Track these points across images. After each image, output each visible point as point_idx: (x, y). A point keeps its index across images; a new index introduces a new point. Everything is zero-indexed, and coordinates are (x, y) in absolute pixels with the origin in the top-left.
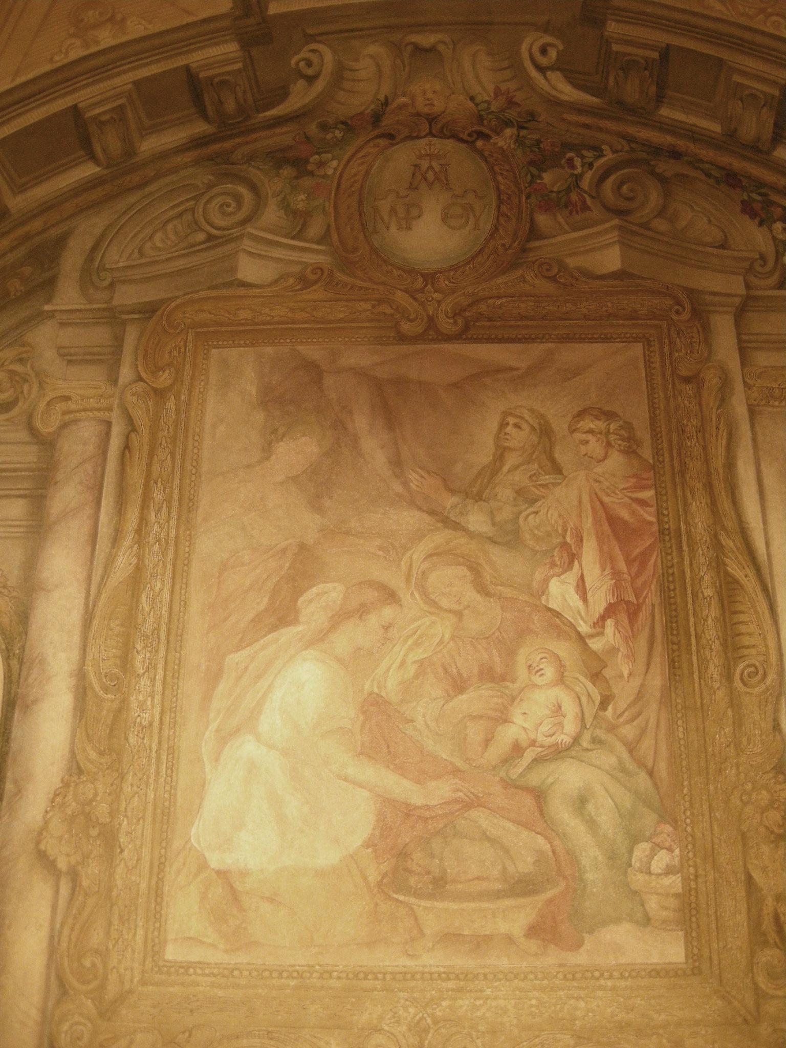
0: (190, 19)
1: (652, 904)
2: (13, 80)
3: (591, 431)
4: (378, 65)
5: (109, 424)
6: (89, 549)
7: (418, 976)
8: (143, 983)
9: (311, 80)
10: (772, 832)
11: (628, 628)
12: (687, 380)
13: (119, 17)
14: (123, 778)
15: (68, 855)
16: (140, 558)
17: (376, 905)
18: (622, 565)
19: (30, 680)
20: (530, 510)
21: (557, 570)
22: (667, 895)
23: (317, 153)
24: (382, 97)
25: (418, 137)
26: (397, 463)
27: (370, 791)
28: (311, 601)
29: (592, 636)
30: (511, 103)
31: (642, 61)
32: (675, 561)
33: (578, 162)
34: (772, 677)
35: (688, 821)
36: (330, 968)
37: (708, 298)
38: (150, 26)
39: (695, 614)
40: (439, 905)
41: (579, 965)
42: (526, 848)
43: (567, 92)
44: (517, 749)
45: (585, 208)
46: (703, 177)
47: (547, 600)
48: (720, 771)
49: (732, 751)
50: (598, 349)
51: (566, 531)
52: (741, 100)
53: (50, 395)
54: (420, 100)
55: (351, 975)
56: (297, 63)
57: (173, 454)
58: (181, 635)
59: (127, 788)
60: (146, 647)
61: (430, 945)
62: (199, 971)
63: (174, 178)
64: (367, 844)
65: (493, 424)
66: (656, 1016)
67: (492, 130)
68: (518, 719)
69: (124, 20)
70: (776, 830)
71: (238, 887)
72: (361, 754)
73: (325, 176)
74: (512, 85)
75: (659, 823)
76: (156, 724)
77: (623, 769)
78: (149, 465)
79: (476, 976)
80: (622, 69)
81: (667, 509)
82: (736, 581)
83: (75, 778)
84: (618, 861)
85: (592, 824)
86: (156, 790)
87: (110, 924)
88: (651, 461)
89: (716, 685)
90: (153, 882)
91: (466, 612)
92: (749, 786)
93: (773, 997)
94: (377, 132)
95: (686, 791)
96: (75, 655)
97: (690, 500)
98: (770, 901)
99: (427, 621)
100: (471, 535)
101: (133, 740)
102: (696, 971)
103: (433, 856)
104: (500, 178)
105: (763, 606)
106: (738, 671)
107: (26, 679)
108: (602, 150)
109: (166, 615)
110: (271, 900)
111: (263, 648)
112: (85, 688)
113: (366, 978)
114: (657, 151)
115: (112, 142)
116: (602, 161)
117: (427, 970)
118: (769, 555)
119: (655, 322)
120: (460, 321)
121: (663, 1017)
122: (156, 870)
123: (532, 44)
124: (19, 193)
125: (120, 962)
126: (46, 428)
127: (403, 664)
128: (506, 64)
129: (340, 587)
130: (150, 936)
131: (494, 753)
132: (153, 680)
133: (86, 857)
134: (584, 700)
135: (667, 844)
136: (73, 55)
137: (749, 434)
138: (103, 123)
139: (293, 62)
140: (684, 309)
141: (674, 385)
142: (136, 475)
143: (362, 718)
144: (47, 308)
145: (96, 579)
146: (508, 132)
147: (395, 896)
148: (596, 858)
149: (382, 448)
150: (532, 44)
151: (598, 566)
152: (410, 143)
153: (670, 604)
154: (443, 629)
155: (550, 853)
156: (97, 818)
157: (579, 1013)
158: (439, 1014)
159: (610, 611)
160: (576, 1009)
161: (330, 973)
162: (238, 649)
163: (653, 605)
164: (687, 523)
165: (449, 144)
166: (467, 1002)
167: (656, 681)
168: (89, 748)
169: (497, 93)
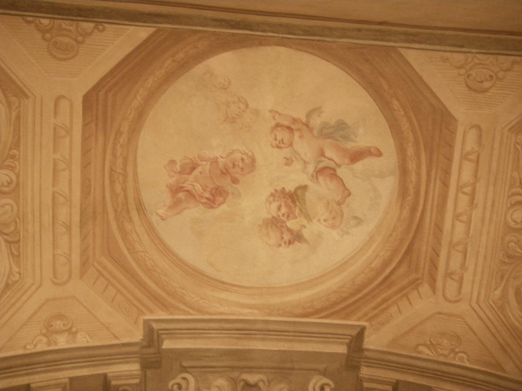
13: (74, 330)
69: (76, 332)
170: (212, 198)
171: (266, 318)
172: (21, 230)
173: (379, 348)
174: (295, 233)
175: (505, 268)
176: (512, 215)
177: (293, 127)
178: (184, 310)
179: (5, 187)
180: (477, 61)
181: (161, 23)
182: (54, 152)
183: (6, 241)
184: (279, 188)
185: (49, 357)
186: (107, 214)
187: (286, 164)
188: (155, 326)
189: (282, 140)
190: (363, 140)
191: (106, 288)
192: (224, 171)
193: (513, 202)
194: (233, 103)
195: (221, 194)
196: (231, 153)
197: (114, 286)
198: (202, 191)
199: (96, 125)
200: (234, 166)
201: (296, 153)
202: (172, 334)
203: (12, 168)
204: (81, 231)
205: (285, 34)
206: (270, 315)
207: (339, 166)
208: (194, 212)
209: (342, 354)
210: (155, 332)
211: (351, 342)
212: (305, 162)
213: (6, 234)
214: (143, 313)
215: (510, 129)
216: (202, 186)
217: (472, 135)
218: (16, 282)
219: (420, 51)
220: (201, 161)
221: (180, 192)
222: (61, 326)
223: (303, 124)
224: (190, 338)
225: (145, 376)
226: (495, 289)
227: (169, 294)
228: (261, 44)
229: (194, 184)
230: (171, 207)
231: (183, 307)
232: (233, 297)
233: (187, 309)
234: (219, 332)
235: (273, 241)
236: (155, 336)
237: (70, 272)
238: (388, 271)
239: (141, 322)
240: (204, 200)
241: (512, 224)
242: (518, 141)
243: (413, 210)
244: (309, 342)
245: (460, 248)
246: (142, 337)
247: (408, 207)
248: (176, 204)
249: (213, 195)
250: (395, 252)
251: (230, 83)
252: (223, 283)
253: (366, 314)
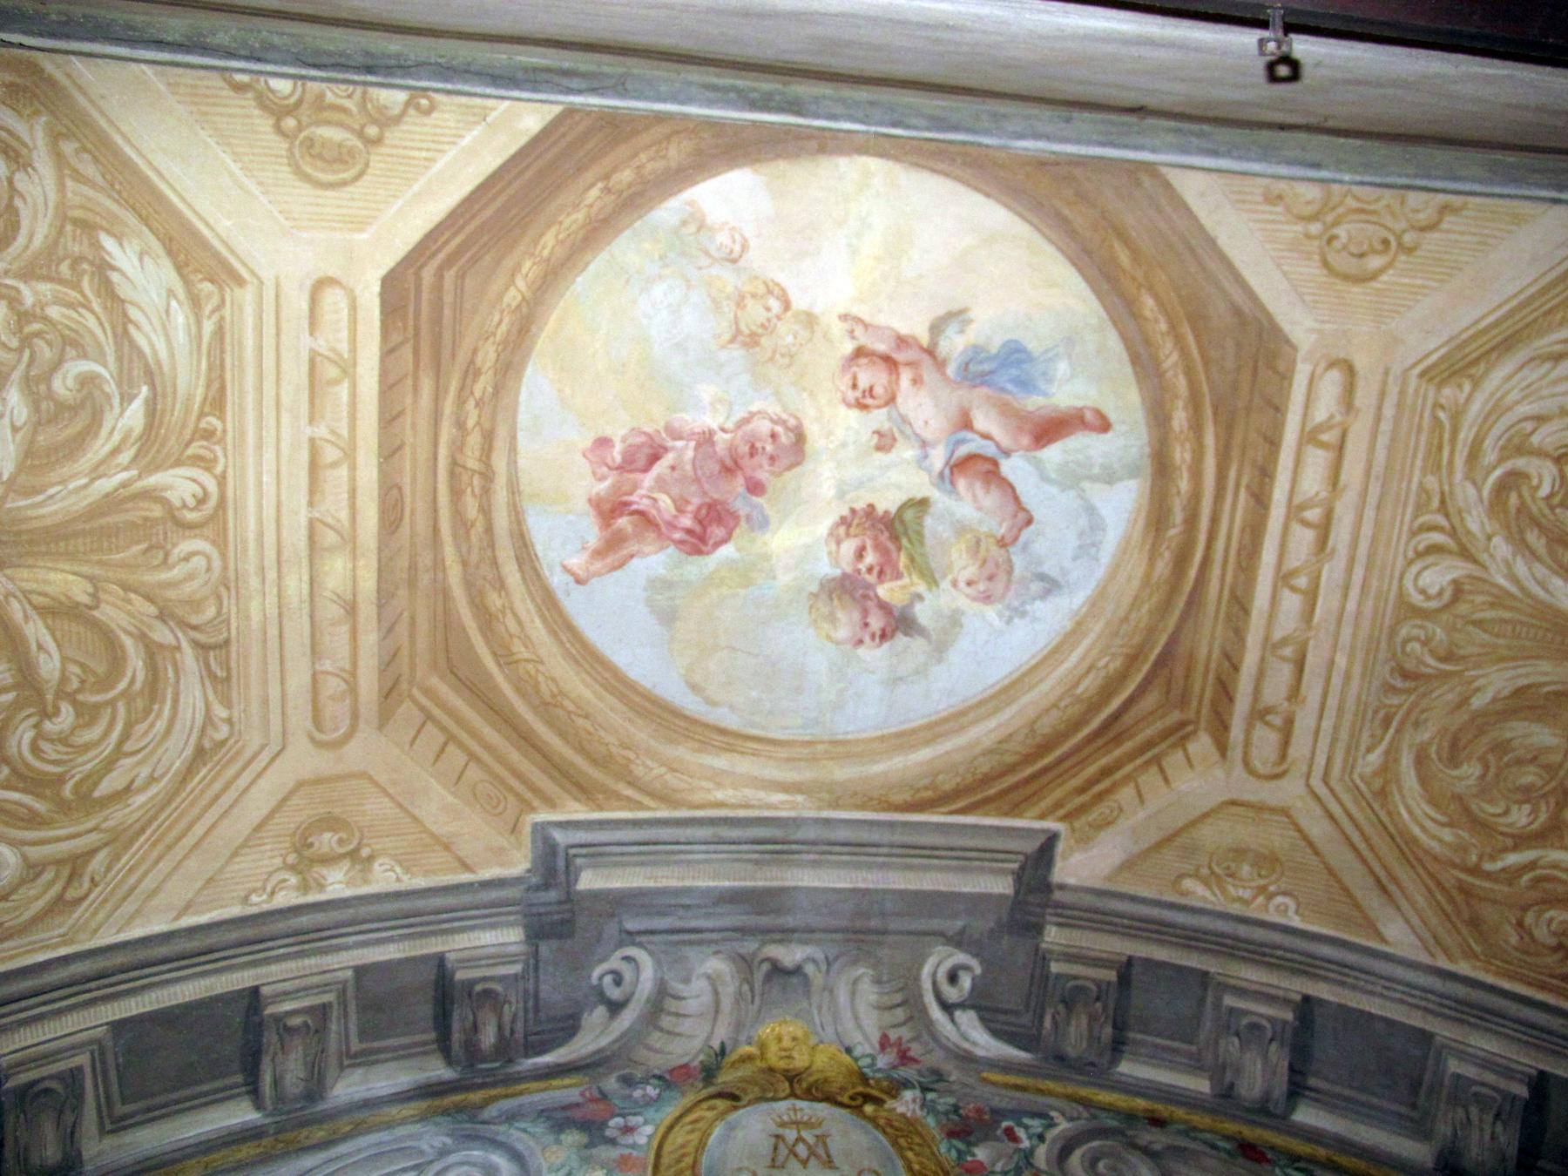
0: (466, 877)
2: (177, 918)
4: (716, 993)
9: (615, 1008)
13: (365, 852)
23: (623, 1116)
24: (716, 1044)
25: (774, 1099)
30: (905, 1058)
31: (1093, 987)
33: (1021, 1133)
38: (405, 878)
43: (983, 1043)
46: (1208, 1150)
52: (1237, 1034)
54: (773, 1048)
56: (601, 978)
63: (384, 1136)
67: (882, 1090)
69: (371, 858)
73: (634, 1146)
74: (905, 1033)
80: (1064, 1001)
94: (712, 1090)
104: (910, 1154)
114: (1130, 1117)
115: (292, 1069)
116: (1055, 1131)
124: (112, 1132)
128: (898, 998)
136: (284, 899)
138: (290, 1030)
146: (908, 1095)
152: (764, 1106)
165: (822, 1110)
169: (884, 1043)
170: (698, 529)
171: (825, 814)
172: (233, 616)
173: (1088, 884)
174: (896, 613)
175: (1396, 701)
176: (1419, 574)
177: (900, 357)
178: (629, 799)
179: (192, 510)
180: (1355, 204)
181: (580, 92)
182: (312, 420)
183: (197, 645)
184: (860, 505)
185: (304, 921)
186: (444, 569)
187: (879, 448)
188: (560, 837)
189: (871, 389)
190: (1066, 390)
191: (442, 750)
192: (728, 462)
193: (1421, 547)
194: (754, 296)
195: (719, 520)
196: (747, 421)
197: (461, 745)
198: (674, 512)
199: (416, 352)
200: (753, 451)
201: (905, 420)
202: (597, 854)
203: (207, 463)
204: (379, 614)
205: (881, 124)
206: (835, 805)
207: (1007, 453)
208: (654, 561)
209: (1002, 896)
210: (561, 855)
211: (1022, 868)
212: (924, 444)
213: (195, 628)
214: (533, 809)
215: (1422, 374)
216: (674, 501)
217: (1331, 385)
218: (223, 743)
219: (1214, 176)
220: (675, 439)
221: (621, 515)
222: (335, 846)
223: (921, 348)
224: (642, 864)
225: (536, 953)
226: (1369, 750)
227: (594, 762)
228: (822, 150)
229: (655, 495)
230: (598, 554)
231: (629, 792)
232: (744, 766)
233: (638, 796)
234: (712, 847)
235: (843, 633)
236: (561, 864)
237: (355, 715)
238: (1115, 704)
239: (528, 829)
240: (678, 535)
241: (1417, 599)
242: (1443, 401)
243: (1181, 560)
244: (926, 868)
245: (1288, 651)
246: (528, 866)
247: (1167, 554)
248: (612, 549)
249: (700, 522)
250: (1133, 659)
251: (745, 247)
252: (723, 732)
253: (1058, 805)
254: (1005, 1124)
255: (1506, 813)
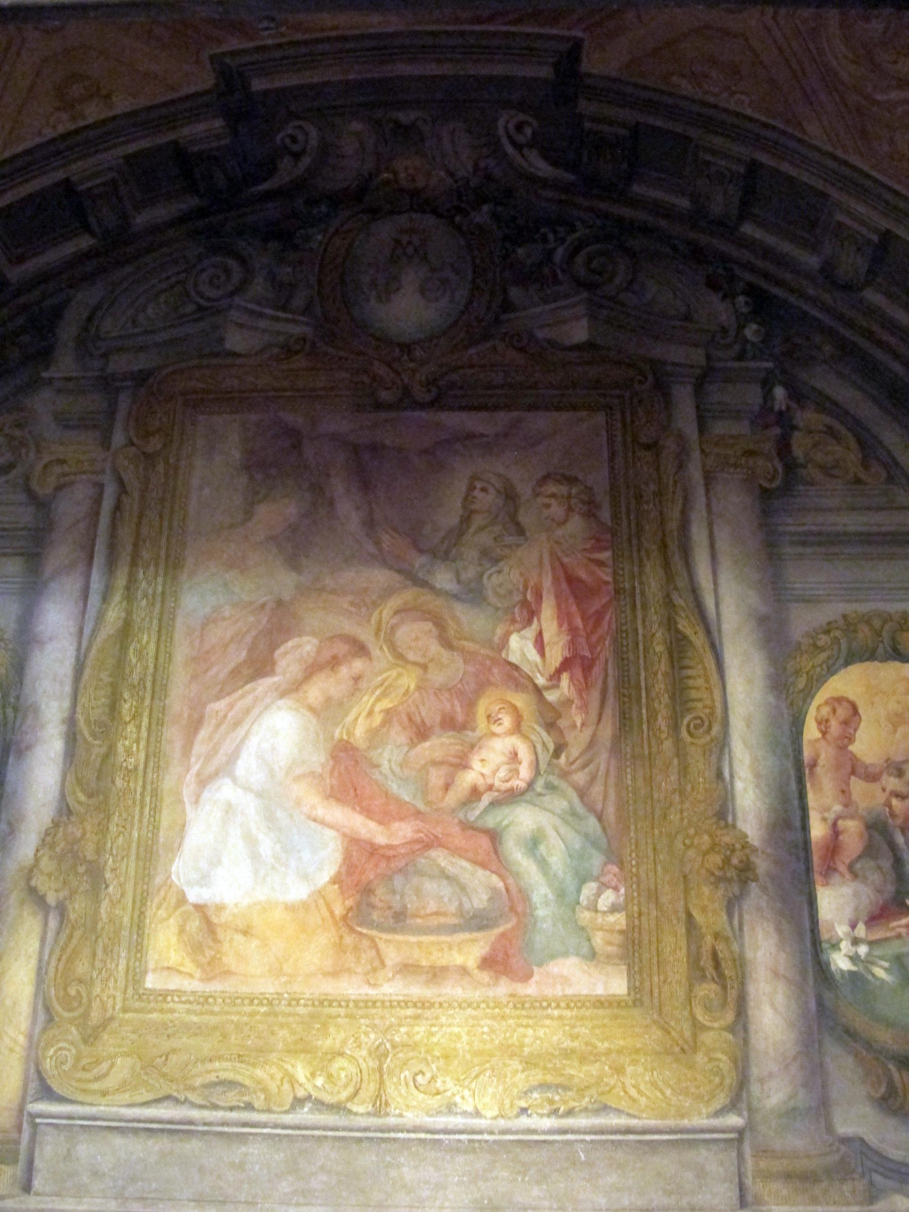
0: (175, 95)
1: (598, 940)
3: (553, 496)
5: (101, 486)
6: (81, 604)
7: (378, 1004)
8: (125, 1010)
9: (297, 156)
10: (713, 874)
11: (582, 680)
12: (648, 447)
14: (109, 819)
15: (56, 891)
16: (129, 613)
17: (341, 938)
18: (579, 622)
19: (24, 728)
20: (494, 569)
21: (517, 626)
22: (612, 931)
26: (370, 524)
27: (338, 830)
28: (285, 654)
29: (548, 688)
30: (489, 177)
32: (629, 618)
33: (551, 237)
34: (716, 729)
35: (634, 863)
36: (297, 996)
37: (669, 368)
39: (646, 669)
40: (399, 937)
41: (528, 996)
42: (481, 885)
43: (542, 168)
44: (475, 793)
45: (556, 281)
47: (507, 654)
48: (665, 816)
49: (677, 798)
50: (564, 416)
51: (526, 588)
53: (46, 459)
54: (402, 175)
55: (316, 1003)
56: (282, 140)
57: (161, 517)
58: (166, 685)
59: (113, 828)
60: (132, 696)
61: (390, 975)
62: (176, 999)
64: (335, 880)
65: (460, 487)
66: (599, 1044)
68: (476, 765)
70: (717, 873)
71: (215, 920)
72: (330, 796)
75: (605, 864)
76: (141, 767)
77: (574, 814)
78: (139, 524)
79: (432, 1005)
81: (623, 569)
82: (685, 637)
83: (65, 818)
84: (566, 899)
85: (543, 865)
86: (140, 829)
87: (94, 954)
88: (609, 524)
89: (664, 736)
90: (136, 916)
91: (430, 665)
92: (692, 831)
93: (709, 1029)
95: (632, 834)
96: (67, 704)
97: (645, 561)
98: (709, 939)
99: (394, 673)
100: (438, 592)
101: (119, 782)
102: (637, 1003)
103: (394, 892)
105: (709, 661)
106: (685, 722)
107: (20, 727)
108: (574, 226)
109: (151, 666)
110: (246, 933)
111: (242, 697)
112: (75, 734)
113: (330, 1005)
117: (386, 998)
118: (718, 614)
119: (618, 392)
120: (434, 390)
121: (606, 1044)
122: (138, 904)
123: (508, 122)
125: (103, 990)
126: (42, 491)
127: (370, 713)
129: (315, 641)
130: (131, 964)
131: (452, 798)
132: (139, 727)
133: (73, 893)
134: (539, 747)
135: (613, 884)
136: (61, 129)
137: (703, 499)
139: (278, 138)
140: (646, 379)
141: (634, 452)
142: (126, 534)
143: (331, 763)
144: (45, 375)
145: (87, 631)
146: (485, 208)
147: (359, 929)
148: (546, 895)
149: (358, 508)
150: (508, 122)
151: (555, 622)
153: (623, 659)
154: (409, 680)
155: (504, 890)
156: (85, 856)
157: (527, 1041)
158: (397, 1039)
159: (566, 665)
160: (525, 1036)
161: (298, 1000)
162: (218, 698)
163: (607, 661)
164: (641, 583)
165: (430, 221)
166: (423, 1029)
167: (607, 731)
168: (78, 790)
169: (476, 168)
254: (543, 230)
255: (895, 62)
